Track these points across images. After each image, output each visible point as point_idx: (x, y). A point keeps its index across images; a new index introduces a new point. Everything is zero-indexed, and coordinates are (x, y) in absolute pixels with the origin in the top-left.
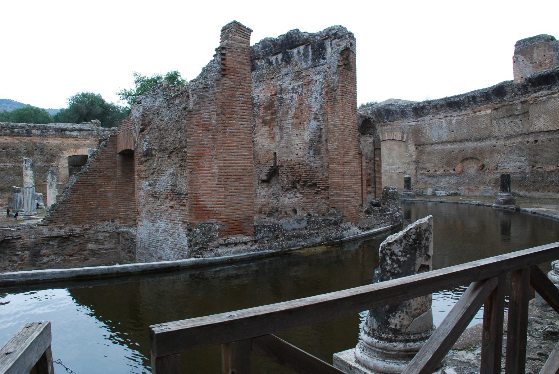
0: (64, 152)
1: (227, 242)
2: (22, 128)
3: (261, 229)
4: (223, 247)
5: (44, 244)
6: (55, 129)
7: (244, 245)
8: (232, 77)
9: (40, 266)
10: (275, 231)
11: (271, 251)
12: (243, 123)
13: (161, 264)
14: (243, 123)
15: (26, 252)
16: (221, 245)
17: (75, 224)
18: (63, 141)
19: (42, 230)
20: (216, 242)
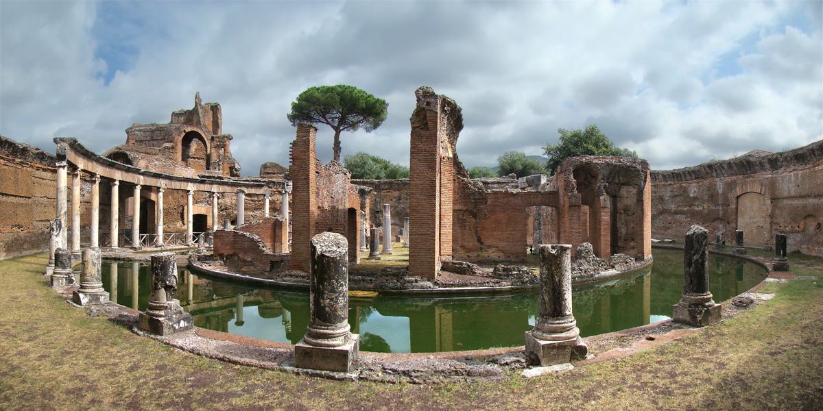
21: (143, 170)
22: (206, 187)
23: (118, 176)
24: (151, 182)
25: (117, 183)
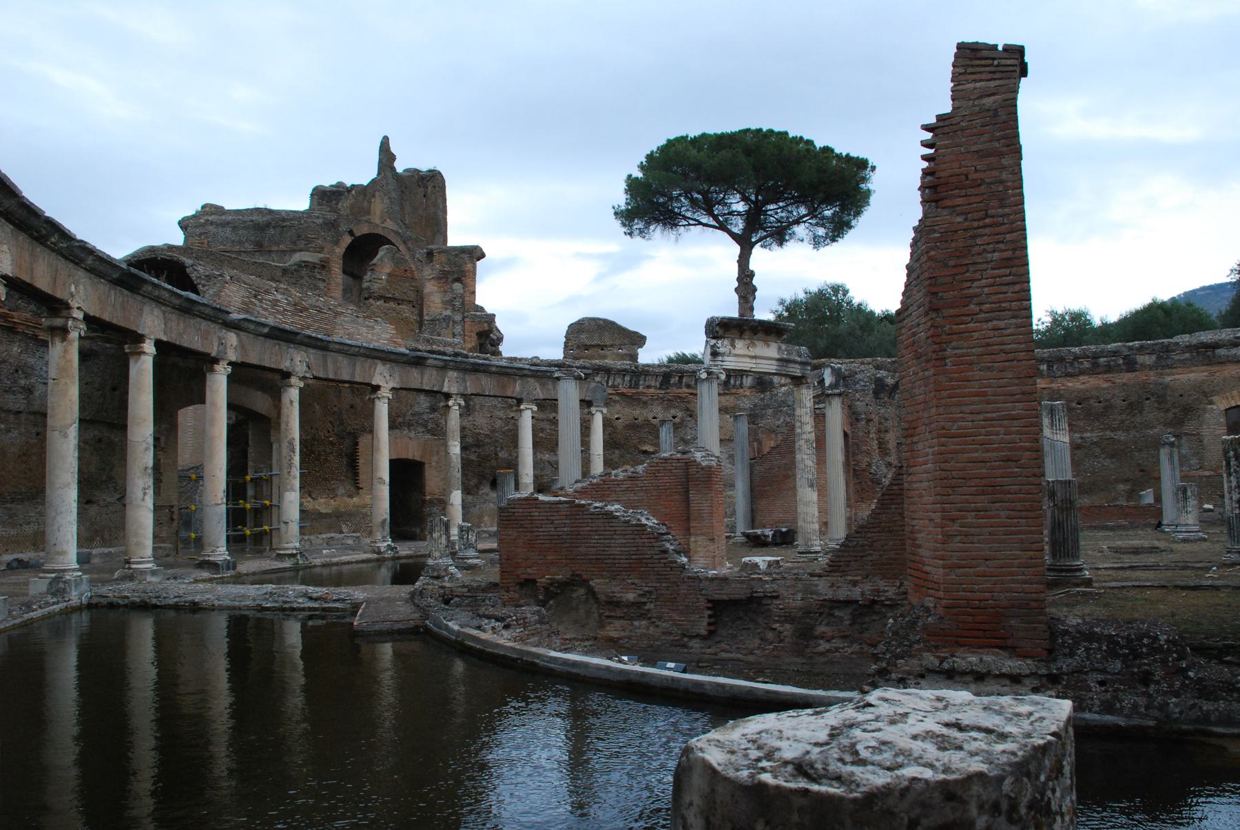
0: (1215, 398)
1: (946, 666)
2: (1115, 353)
3: (1077, 643)
4: (936, 677)
5: (821, 614)
6: (1190, 348)
7: (1008, 682)
8: (959, 201)
9: (811, 658)
10: (1137, 656)
11: (1109, 718)
12: (1001, 324)
13: (768, 692)
14: (1001, 324)
15: (788, 626)
16: (930, 671)
17: (884, 577)
18: (1212, 374)
19: (816, 585)
20: (915, 661)
21: (235, 316)
22: (427, 379)
23: (153, 325)
24: (263, 354)
25: (149, 347)
